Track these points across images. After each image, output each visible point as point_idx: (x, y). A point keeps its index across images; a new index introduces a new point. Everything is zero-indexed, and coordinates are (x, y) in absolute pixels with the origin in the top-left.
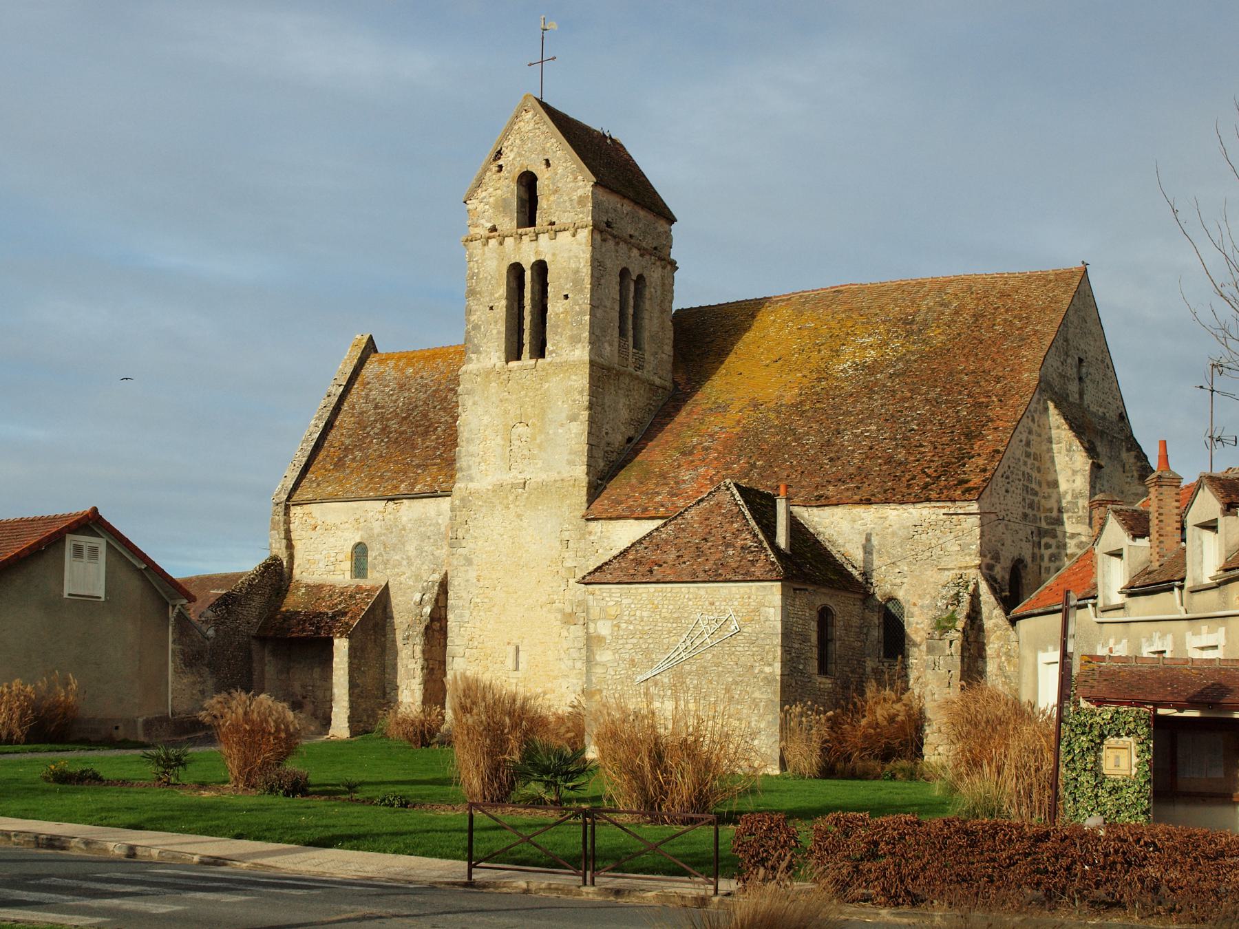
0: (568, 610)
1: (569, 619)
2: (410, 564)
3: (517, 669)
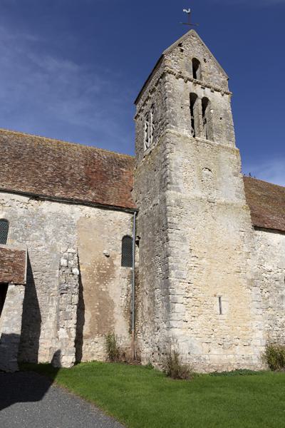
0: (250, 276)
1: (252, 283)
2: (47, 240)
3: (221, 313)
